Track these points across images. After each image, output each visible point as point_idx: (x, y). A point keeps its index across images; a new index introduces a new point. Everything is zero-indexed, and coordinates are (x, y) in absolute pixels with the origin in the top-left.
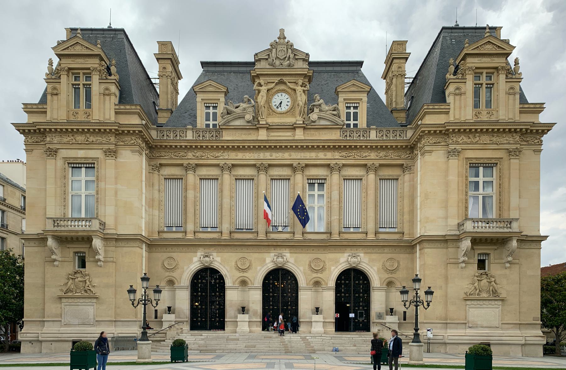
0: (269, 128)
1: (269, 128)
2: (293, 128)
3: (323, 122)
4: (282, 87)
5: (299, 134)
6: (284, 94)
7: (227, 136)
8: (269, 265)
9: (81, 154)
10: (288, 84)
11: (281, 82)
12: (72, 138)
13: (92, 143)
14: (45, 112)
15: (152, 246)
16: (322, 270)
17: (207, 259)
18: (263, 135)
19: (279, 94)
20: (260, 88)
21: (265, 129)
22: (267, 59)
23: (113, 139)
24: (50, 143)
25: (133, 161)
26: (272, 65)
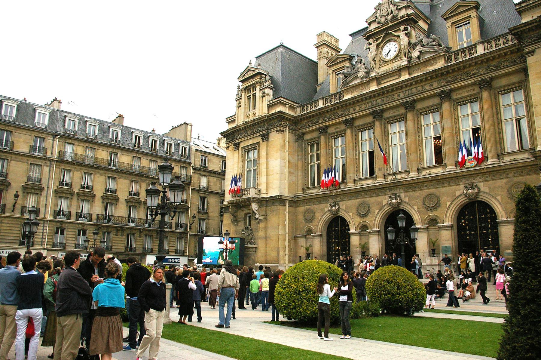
0: (378, 79)
2: (399, 71)
6: (391, 43)
10: (394, 33)
11: (388, 34)
15: (295, 202)
16: (437, 206)
18: (374, 87)
19: (388, 44)
20: (370, 46)
22: (375, 21)
26: (379, 23)
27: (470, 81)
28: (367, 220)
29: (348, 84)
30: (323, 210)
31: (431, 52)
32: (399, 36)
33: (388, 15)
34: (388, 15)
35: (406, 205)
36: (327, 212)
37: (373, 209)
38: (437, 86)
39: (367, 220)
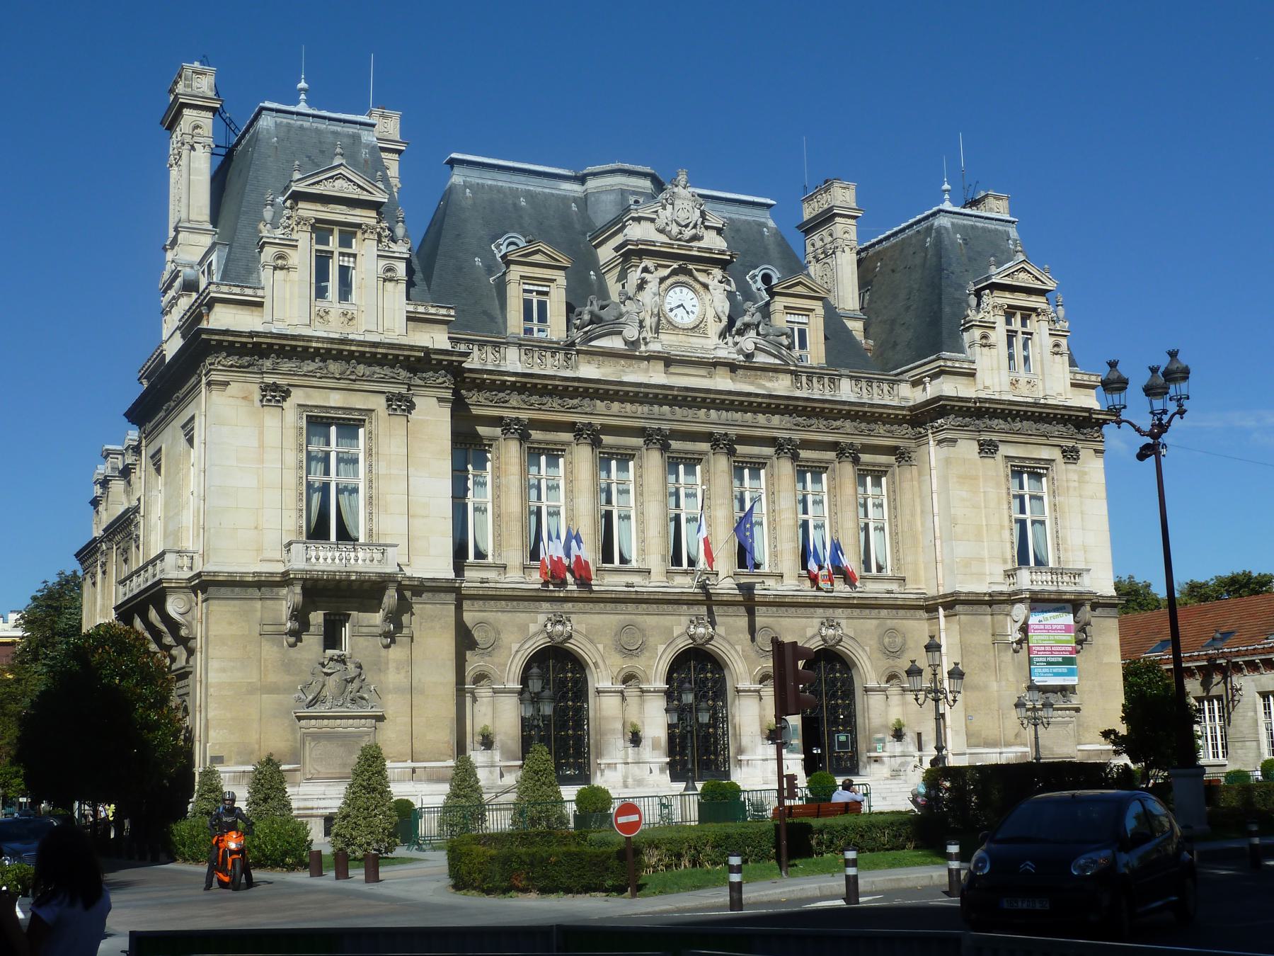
0: (669, 361)
1: (669, 361)
2: (714, 365)
3: (761, 359)
4: (682, 278)
5: (723, 382)
6: (685, 290)
7: (588, 370)
8: (678, 641)
9: (335, 399)
10: (695, 273)
12: (321, 364)
13: (361, 379)
14: (260, 305)
17: (559, 628)
18: (656, 376)
19: (677, 289)
21: (662, 363)
23: (404, 374)
24: (273, 371)
25: (434, 414)
27: (830, 438)
28: (638, 664)
29: (591, 340)
30: (523, 628)
31: (775, 356)
32: (706, 286)
33: (686, 226)
34: (686, 226)
35: (721, 641)
36: (535, 634)
37: (652, 641)
38: (777, 425)
39: (638, 664)
